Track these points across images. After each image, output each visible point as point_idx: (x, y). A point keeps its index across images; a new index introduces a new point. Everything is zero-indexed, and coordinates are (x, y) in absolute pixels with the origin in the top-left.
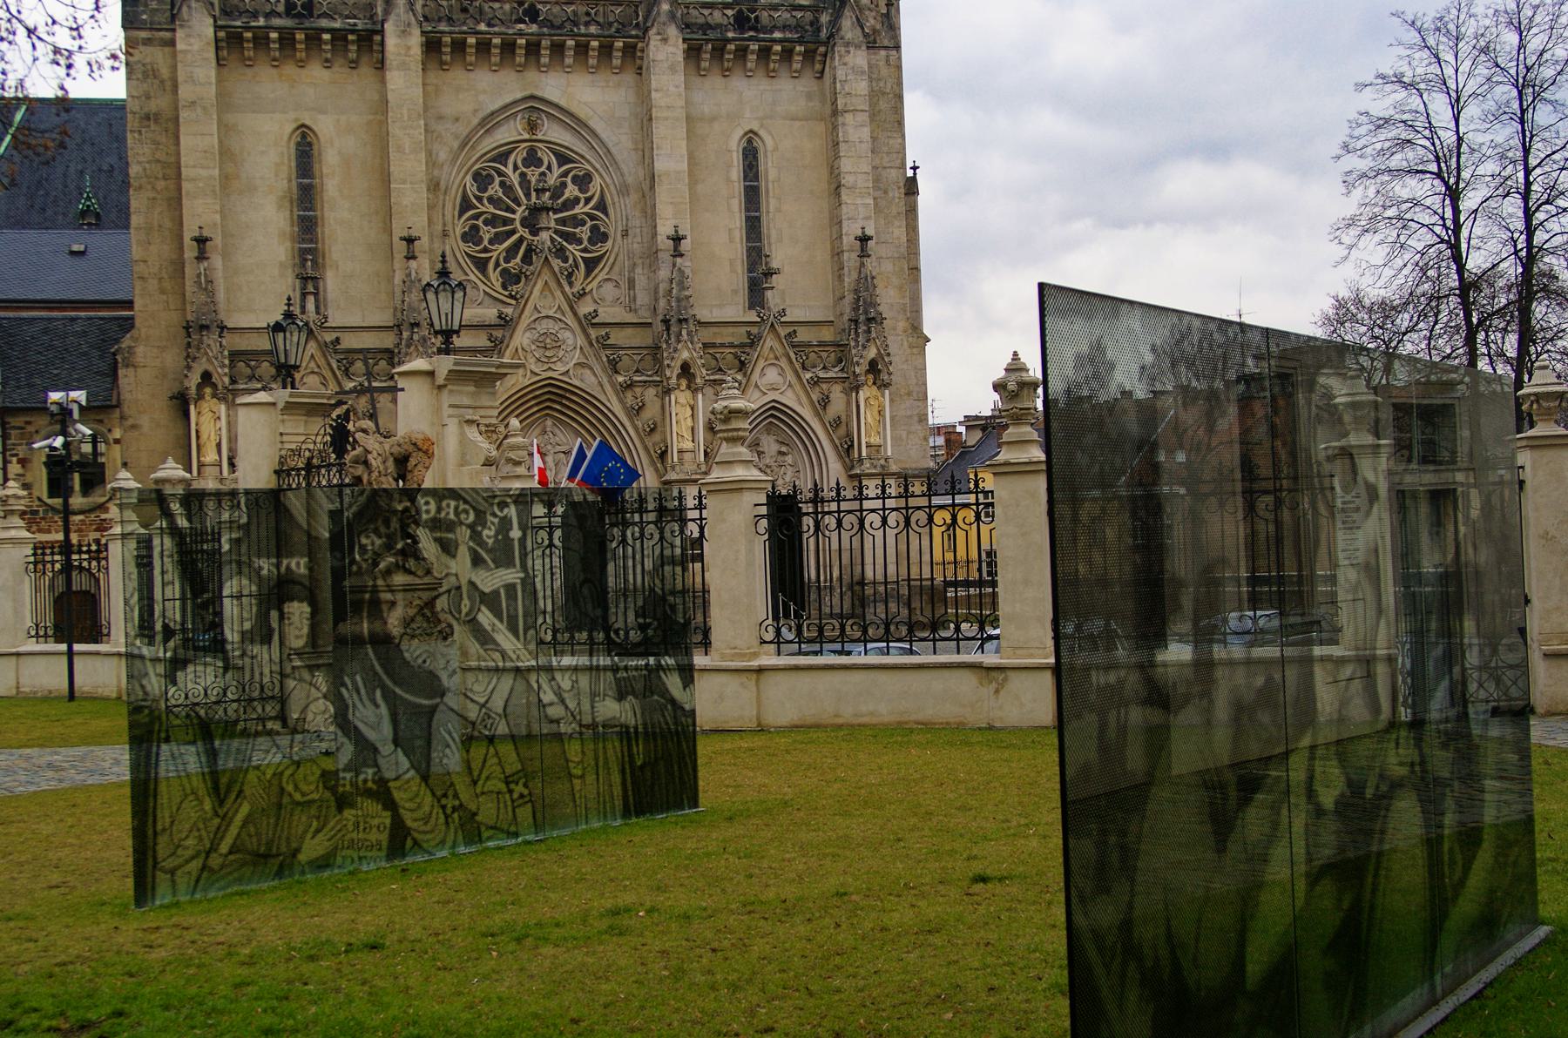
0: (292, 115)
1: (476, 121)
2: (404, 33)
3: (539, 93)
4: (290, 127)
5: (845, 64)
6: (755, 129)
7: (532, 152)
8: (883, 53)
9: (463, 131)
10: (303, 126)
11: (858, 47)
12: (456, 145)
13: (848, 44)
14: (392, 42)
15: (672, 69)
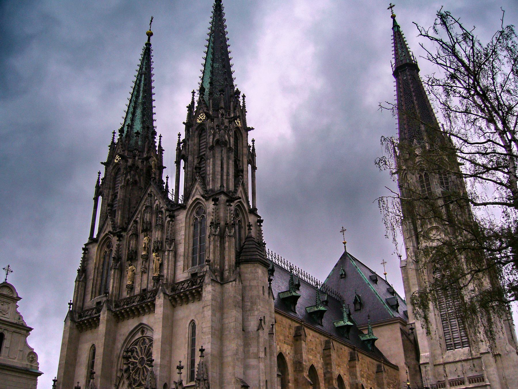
0: (92, 342)
1: (127, 334)
2: (104, 313)
3: (142, 322)
4: (91, 345)
5: (205, 291)
6: (193, 318)
7: (144, 339)
8: (231, 283)
9: (124, 337)
10: (93, 345)
11: (209, 284)
12: (122, 342)
13: (206, 285)
14: (101, 316)
15: (160, 306)
